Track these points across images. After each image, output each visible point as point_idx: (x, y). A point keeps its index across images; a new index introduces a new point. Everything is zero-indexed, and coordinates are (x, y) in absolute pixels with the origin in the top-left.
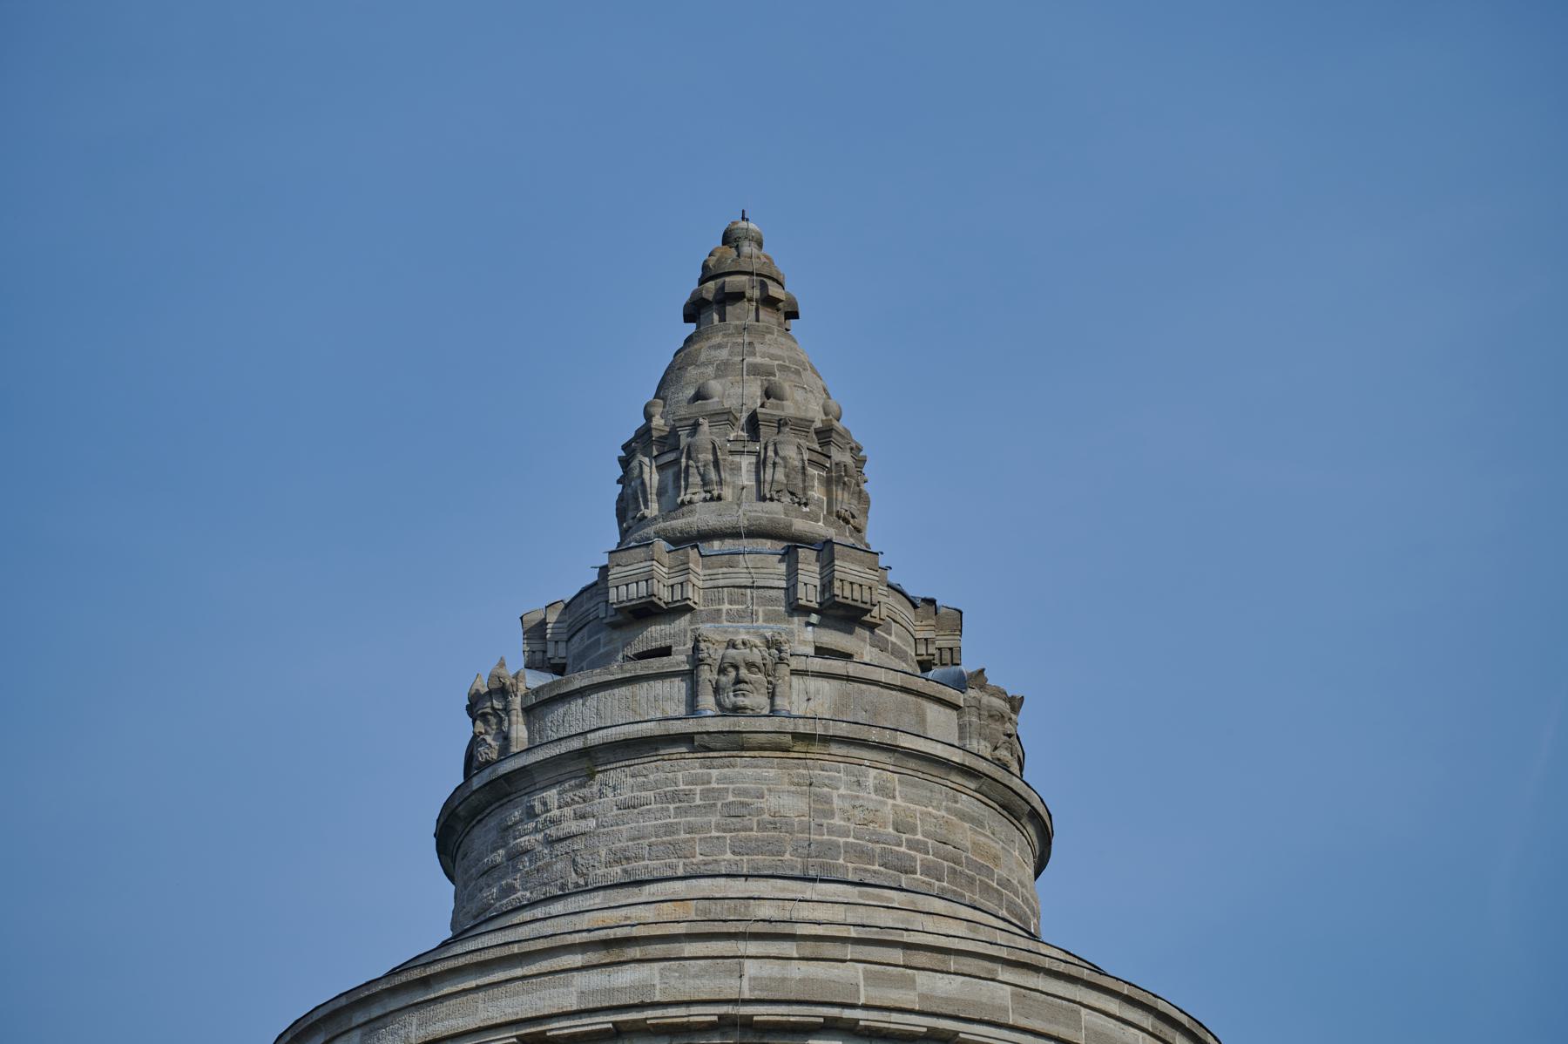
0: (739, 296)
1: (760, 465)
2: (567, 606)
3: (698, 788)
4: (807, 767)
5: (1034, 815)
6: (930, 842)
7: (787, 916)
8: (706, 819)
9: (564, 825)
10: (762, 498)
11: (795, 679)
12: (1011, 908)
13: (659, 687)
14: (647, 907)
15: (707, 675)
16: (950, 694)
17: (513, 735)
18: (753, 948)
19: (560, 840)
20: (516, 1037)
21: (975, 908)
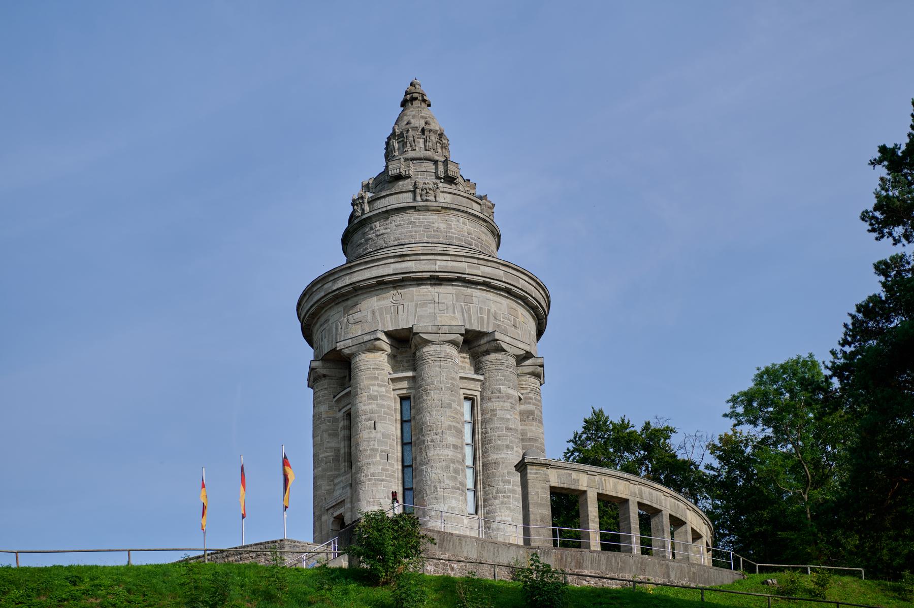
0: (416, 99)
1: (425, 141)
2: (375, 179)
3: (417, 221)
4: (445, 216)
10: (427, 150)
11: (441, 193)
13: (405, 195)
15: (418, 191)
16: (479, 201)
17: (365, 209)
19: (380, 235)
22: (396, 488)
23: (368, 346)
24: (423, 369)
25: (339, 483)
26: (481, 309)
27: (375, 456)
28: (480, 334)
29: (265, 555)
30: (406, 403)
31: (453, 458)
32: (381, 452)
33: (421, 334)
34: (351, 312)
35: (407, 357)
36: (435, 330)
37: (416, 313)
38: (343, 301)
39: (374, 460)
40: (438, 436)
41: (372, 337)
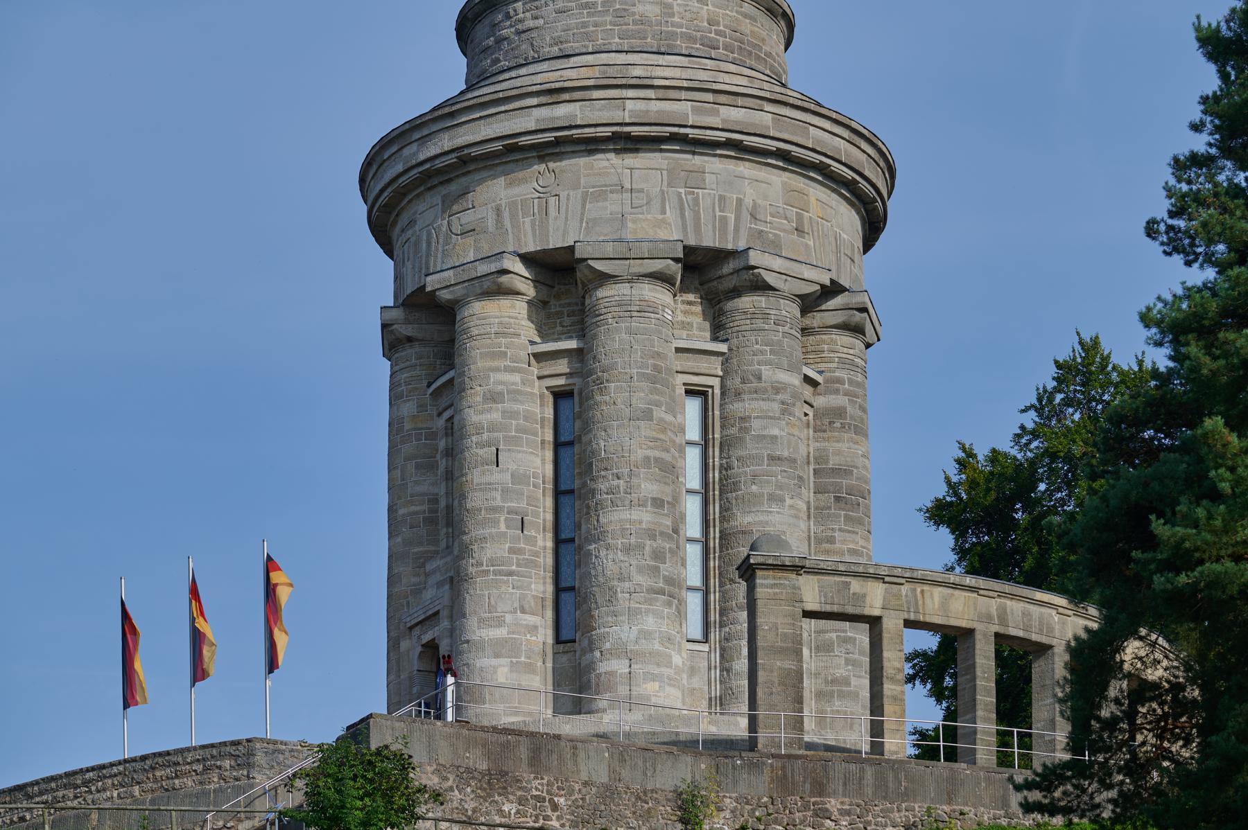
5: (785, 15)
6: (727, 31)
7: (649, 75)
8: (604, 19)
9: (526, 23)
12: (772, 68)
14: (572, 70)
18: (631, 93)
19: (524, 32)
20: (502, 146)
21: (752, 69)
22: (541, 588)
23: (485, 287)
24: (595, 335)
25: (434, 572)
26: (722, 198)
27: (496, 522)
28: (720, 256)
29: (220, 768)
30: (565, 404)
31: (652, 527)
32: (508, 513)
33: (590, 262)
34: (455, 208)
35: (569, 304)
36: (622, 250)
37: (583, 214)
38: (441, 183)
39: (493, 530)
40: (622, 481)
41: (493, 267)
